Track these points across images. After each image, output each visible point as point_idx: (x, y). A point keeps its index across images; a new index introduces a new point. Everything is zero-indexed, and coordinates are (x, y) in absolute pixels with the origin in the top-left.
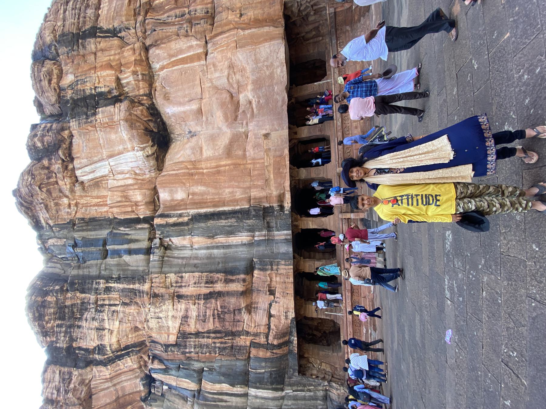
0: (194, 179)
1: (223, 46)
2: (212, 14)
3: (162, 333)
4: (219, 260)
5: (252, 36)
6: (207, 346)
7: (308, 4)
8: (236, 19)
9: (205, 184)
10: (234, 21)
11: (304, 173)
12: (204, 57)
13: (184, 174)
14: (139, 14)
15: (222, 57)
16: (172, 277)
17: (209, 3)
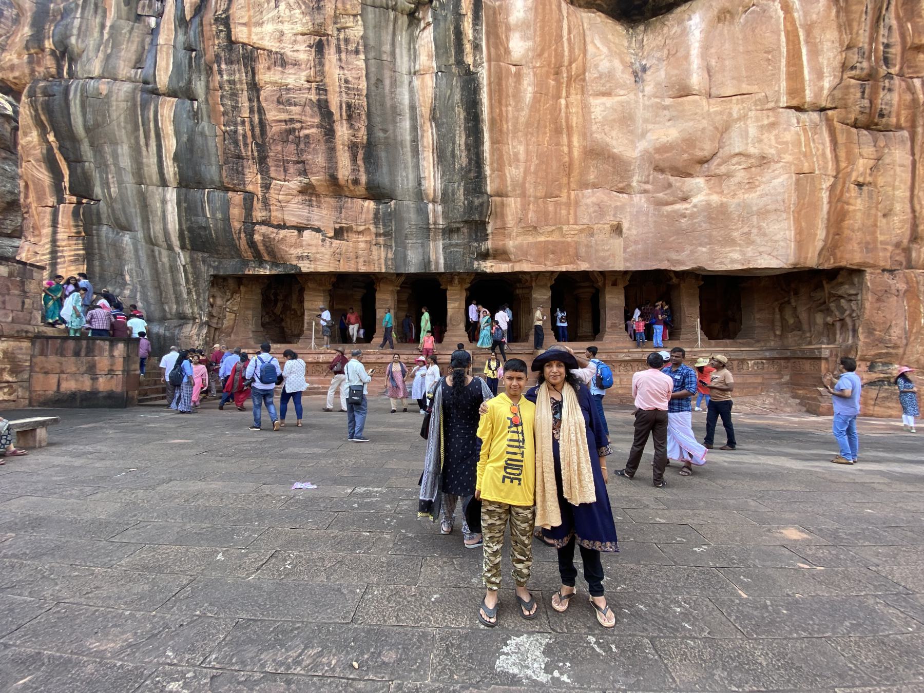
0: (548, 77)
1: (807, 145)
3: (249, 10)
4: (391, 132)
5: (815, 206)
6: (235, 108)
7: (848, 312)
8: (854, 175)
9: (536, 100)
10: (852, 170)
11: (542, 296)
12: (794, 103)
13: (559, 55)
15: (786, 143)
16: (356, 31)
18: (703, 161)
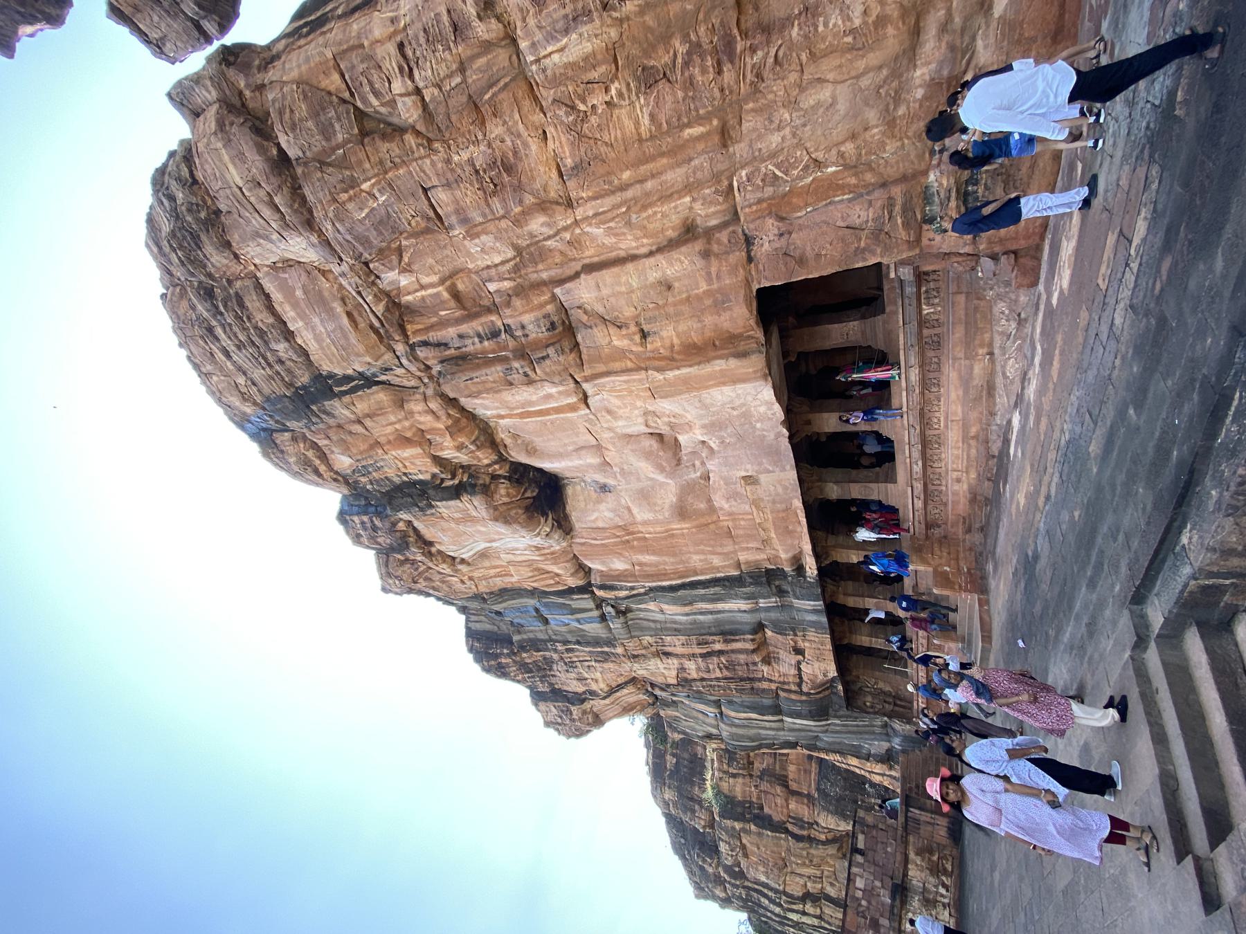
0: (633, 547)
1: (619, 391)
2: (563, 322)
9: (654, 553)
12: (583, 406)
13: (615, 544)
14: (390, 338)
16: (648, 639)
17: (547, 303)
18: (660, 437)
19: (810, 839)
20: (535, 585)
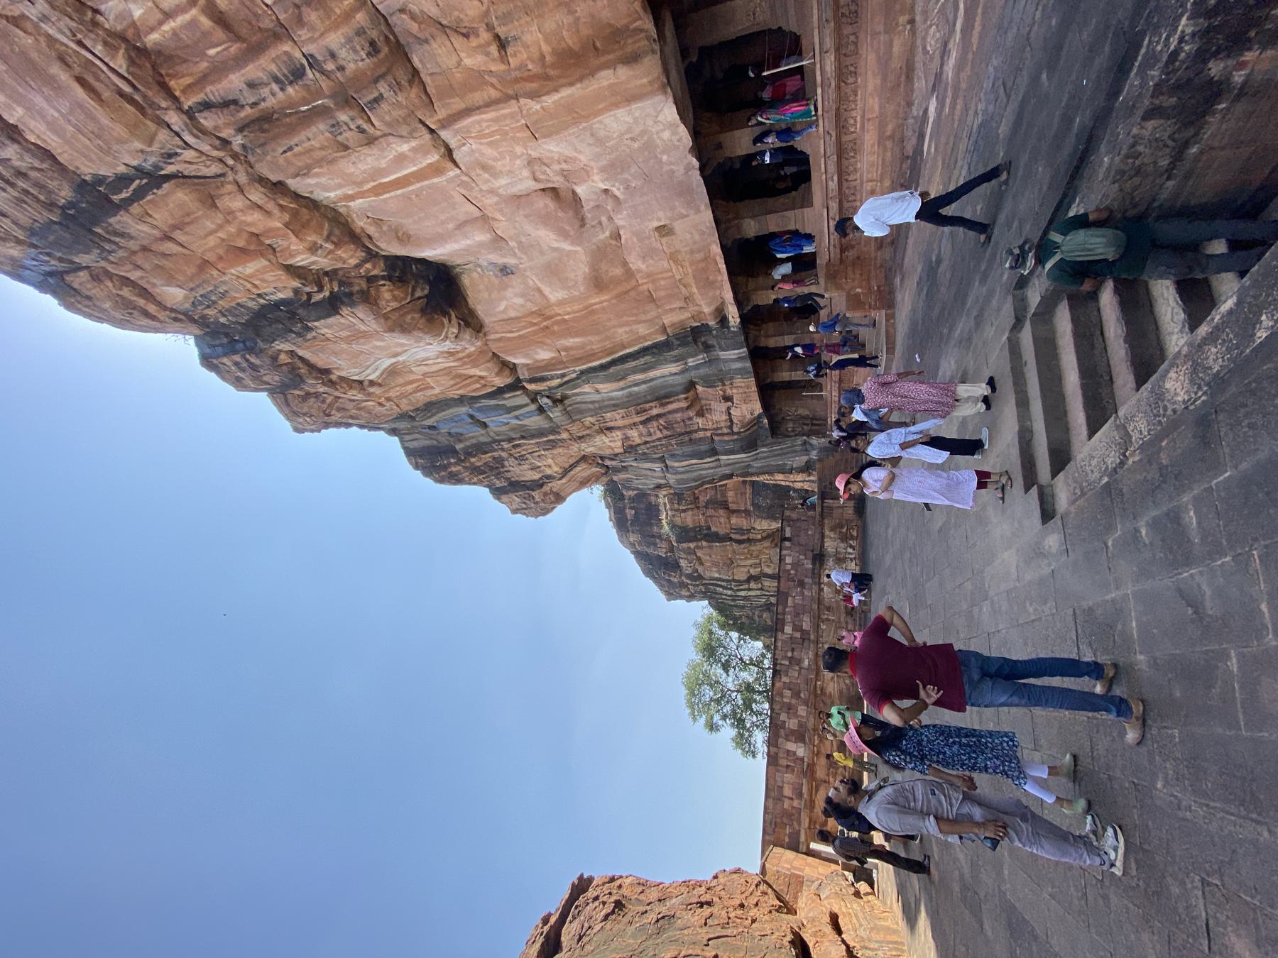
0: (554, 333)
2: (387, 38)
9: (577, 335)
12: (450, 165)
13: (535, 333)
16: (589, 420)
18: (554, 192)
19: (749, 540)
20: (461, 392)
